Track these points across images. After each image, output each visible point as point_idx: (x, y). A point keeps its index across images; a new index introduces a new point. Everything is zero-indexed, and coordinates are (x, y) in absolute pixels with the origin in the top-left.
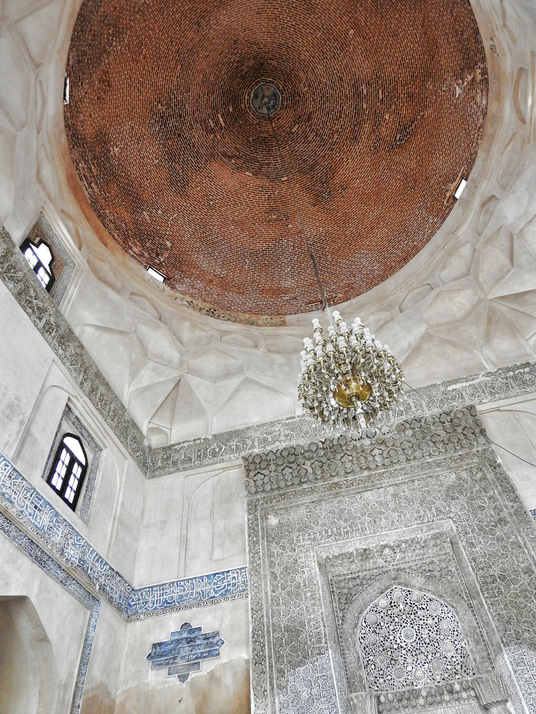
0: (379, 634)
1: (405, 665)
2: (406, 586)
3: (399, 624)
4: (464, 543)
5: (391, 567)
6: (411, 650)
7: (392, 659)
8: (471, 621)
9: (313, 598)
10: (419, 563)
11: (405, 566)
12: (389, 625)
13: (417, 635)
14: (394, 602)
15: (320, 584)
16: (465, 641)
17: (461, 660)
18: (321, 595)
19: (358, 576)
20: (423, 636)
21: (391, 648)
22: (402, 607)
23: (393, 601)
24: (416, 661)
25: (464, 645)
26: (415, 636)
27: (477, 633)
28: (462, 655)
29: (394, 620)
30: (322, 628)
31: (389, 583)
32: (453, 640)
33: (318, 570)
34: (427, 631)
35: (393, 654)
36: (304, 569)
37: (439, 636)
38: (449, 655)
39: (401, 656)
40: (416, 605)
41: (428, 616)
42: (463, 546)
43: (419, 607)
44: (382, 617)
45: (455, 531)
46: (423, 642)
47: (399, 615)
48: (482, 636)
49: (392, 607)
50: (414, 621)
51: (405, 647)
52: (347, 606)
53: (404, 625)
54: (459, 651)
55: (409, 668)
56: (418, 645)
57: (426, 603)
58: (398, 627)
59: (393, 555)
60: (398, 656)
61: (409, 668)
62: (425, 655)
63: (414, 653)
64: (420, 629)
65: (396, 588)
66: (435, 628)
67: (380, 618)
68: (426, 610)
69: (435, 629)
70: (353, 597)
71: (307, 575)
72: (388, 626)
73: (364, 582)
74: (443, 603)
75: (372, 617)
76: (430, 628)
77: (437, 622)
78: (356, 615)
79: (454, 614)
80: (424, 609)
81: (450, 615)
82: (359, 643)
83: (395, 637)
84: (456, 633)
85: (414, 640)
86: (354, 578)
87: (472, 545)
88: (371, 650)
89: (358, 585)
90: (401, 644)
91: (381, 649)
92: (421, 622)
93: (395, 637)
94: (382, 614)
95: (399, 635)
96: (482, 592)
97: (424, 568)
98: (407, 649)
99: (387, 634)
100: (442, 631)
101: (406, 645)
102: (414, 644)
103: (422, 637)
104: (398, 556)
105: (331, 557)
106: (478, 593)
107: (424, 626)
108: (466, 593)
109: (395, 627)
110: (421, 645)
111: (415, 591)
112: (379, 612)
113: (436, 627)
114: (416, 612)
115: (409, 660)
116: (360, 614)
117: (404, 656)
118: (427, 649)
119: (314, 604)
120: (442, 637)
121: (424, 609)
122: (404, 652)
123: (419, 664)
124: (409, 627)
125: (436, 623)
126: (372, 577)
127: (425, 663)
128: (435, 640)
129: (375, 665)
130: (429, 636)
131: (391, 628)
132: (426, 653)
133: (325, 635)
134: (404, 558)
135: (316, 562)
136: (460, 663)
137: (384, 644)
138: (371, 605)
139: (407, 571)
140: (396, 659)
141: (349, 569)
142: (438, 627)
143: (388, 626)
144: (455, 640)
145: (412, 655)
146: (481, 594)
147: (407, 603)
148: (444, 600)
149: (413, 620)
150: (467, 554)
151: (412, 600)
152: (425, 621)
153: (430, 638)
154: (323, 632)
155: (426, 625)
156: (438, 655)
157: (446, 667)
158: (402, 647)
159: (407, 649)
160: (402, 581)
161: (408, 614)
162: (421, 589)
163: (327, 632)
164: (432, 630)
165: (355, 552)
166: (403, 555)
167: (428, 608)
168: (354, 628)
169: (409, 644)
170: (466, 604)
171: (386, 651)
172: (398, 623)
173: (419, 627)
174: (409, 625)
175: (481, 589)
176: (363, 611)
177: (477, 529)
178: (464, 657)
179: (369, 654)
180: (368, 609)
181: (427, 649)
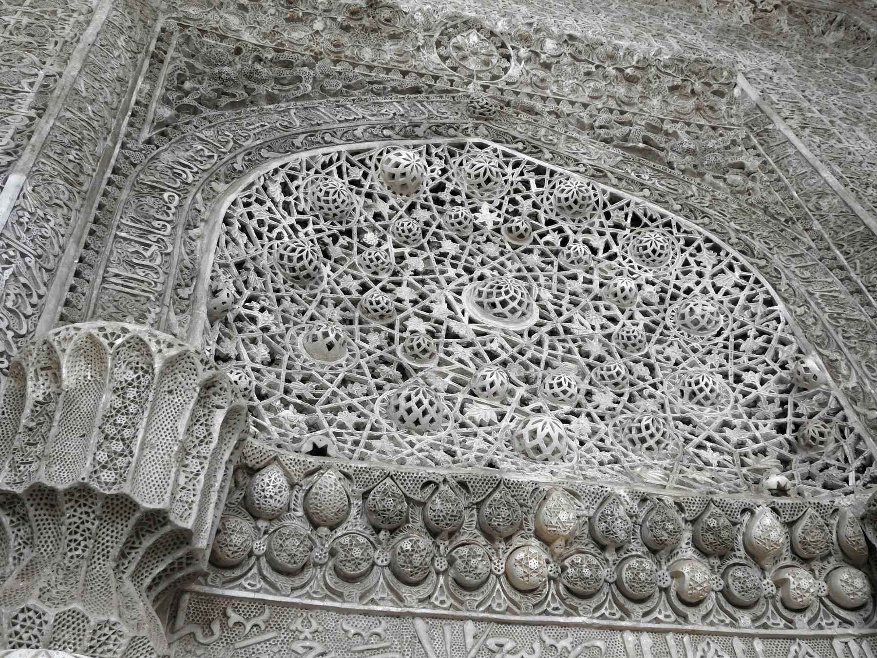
2: (536, 151)
23: (450, 186)
32: (731, 368)
37: (659, 347)
40: (560, 230)
44: (378, 216)
49: (439, 202)
65: (481, 146)
68: (601, 255)
72: (400, 258)
90: (455, 327)
112: (369, 195)
116: (270, 148)
131: (417, 263)
140: (406, 362)
142: (655, 317)
144: (747, 370)
158: (450, 335)
159: (482, 350)
167: (615, 249)
176: (294, 149)
180: (320, 154)
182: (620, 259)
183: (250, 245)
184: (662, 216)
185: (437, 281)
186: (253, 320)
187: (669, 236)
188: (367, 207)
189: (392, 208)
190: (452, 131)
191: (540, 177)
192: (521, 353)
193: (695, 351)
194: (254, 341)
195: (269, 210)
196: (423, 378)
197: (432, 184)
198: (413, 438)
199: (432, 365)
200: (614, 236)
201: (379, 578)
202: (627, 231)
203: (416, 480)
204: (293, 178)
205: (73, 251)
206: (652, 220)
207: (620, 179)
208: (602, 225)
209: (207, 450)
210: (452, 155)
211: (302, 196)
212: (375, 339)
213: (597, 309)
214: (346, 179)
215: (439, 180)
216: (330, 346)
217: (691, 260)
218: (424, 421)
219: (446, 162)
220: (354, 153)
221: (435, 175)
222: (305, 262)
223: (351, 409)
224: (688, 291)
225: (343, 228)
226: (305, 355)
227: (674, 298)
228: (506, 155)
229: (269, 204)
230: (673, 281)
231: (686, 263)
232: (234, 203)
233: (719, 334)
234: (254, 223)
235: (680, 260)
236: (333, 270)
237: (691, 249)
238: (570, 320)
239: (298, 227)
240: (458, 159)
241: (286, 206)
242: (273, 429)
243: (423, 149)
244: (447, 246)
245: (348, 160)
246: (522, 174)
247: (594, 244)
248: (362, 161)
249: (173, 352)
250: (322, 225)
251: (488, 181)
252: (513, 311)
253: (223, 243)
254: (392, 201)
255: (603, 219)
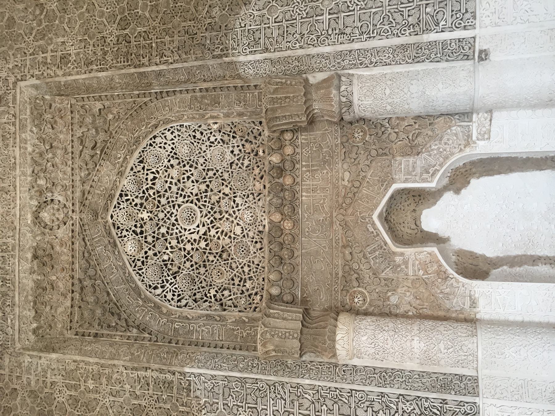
0: (179, 268)
1: (233, 236)
2: (111, 197)
3: (171, 227)
4: (60, 72)
5: (76, 216)
6: (212, 218)
7: (220, 256)
8: (182, 101)
9: (97, 377)
10: (79, 162)
11: (78, 190)
12: (169, 246)
13: (192, 202)
14: (136, 226)
15: (78, 358)
16: (211, 121)
17: (238, 138)
18: (96, 360)
19: (80, 281)
20: (194, 192)
21: (205, 253)
22: (145, 215)
23: (133, 228)
24: (230, 215)
25: (215, 127)
26: (193, 205)
27: (203, 97)
28: (231, 134)
29: (163, 235)
30: (149, 373)
31: (101, 227)
32: (208, 143)
33: (54, 356)
34: (189, 184)
35: (214, 251)
36: (49, 380)
37: (199, 165)
38: (229, 157)
39: (219, 238)
40: (147, 189)
41: (166, 174)
42: (64, 75)
43: (150, 185)
44: (155, 255)
45: (38, 82)
46: (203, 195)
47: (158, 225)
48: (207, 90)
50: (170, 200)
51: (205, 228)
52: (124, 316)
53: (173, 219)
54: (226, 138)
55: (238, 230)
56: (207, 204)
57: (146, 172)
58: (175, 231)
59: (56, 206)
60: (217, 245)
61: (238, 230)
62: (223, 198)
63: (218, 216)
64: (183, 194)
66: (185, 168)
67: (156, 258)
68: (157, 175)
69: (187, 168)
70: (111, 300)
71: (58, 379)
72: (172, 247)
73: (91, 272)
74: (147, 141)
75: (151, 274)
76: (185, 176)
77: (177, 161)
78: (141, 303)
79: (168, 127)
80: (155, 178)
81: (169, 136)
82: (186, 309)
83: (189, 241)
84: (198, 135)
85: (198, 210)
86: (82, 289)
87: (65, 59)
88: (201, 290)
89: (93, 286)
90: (201, 232)
91: (202, 270)
92: (174, 188)
93: (189, 241)
94: (150, 253)
95: (187, 233)
96: (139, 66)
97: (88, 158)
98: (210, 226)
99: (183, 253)
100: (192, 158)
101: (204, 225)
102: (204, 213)
103: (197, 195)
104: (58, 197)
105: (35, 325)
106: (141, 73)
107: (181, 186)
108: (138, 96)
109: (174, 235)
110: (208, 200)
111: (121, 186)
112: (146, 258)
113: (184, 166)
114: (158, 192)
115: (225, 226)
116: (140, 295)
117: (219, 234)
118: (216, 191)
119: (109, 378)
120: (201, 160)
121: (155, 178)
122: (213, 232)
123: (234, 212)
124: (179, 213)
125: (179, 163)
126: (86, 255)
127: (234, 201)
128: (204, 174)
129: (225, 289)
130: (197, 181)
131: (174, 243)
132: (221, 195)
133: (161, 371)
134: (65, 188)
135: (41, 354)
136: (243, 142)
137: (196, 263)
138: (131, 270)
139: (88, 188)
140: (220, 250)
141: (64, 295)
142: (185, 162)
143: (172, 247)
144: (209, 140)
145: (220, 219)
146: (142, 70)
147: (141, 205)
148: (144, 138)
149: (169, 202)
150: (78, 73)
151: (137, 194)
152: (173, 181)
153: (201, 180)
154: (155, 374)
155: (179, 181)
156: (226, 176)
157: (244, 168)
158: (205, 234)
159: (210, 226)
160: (101, 202)
161: (158, 207)
162: (121, 174)
163: (156, 366)
164: (189, 174)
165: (35, 277)
166: (59, 188)
167: (154, 170)
168: (161, 312)
169: (203, 220)
170: (155, 102)
171: (207, 263)
172: (168, 228)
173: (181, 195)
174: (174, 211)
175: (135, 67)
176: (137, 286)
177: (41, 42)
178: (234, 132)
179: (206, 295)
180: (136, 278)
181: (216, 191)
182: (158, 170)
183: (185, 298)
184: (140, 153)
185: (181, 236)
186: (215, 296)
187: (148, 151)
188: (152, 259)
189: (150, 249)
190: (107, 228)
191: (124, 195)
192: (209, 212)
193: (200, 153)
194: (223, 295)
195: (167, 292)
196: (226, 245)
197: (134, 235)
198: (252, 252)
199: (220, 242)
200: (148, 170)
201: (292, 261)
202: (146, 165)
203: (270, 255)
204: (150, 286)
205: (205, 349)
206: (141, 156)
207: (122, 166)
208: (143, 174)
209: (281, 313)
210: (118, 228)
211: (156, 282)
212: (211, 258)
213: (184, 182)
214: (142, 267)
215: (131, 232)
216: (221, 274)
217: (159, 145)
218: (247, 249)
219: (123, 230)
220: (131, 265)
221: (130, 234)
222: (189, 281)
223: (242, 268)
224: (173, 149)
225: (164, 267)
226: (223, 280)
227: (175, 154)
228: (115, 207)
229: (164, 293)
230: (168, 153)
231: (160, 147)
232: (170, 305)
233: (193, 143)
234: (175, 298)
235: (159, 149)
236: (183, 269)
237: (154, 145)
238: (192, 193)
239: (169, 282)
240: (120, 225)
241: (162, 287)
242: (255, 290)
243: (120, 239)
244: (163, 230)
245: (135, 267)
246: (123, 202)
247: (152, 177)
248: (133, 262)
249: (263, 326)
250: (165, 274)
251: (130, 215)
252: (194, 214)
253: (190, 308)
254: (147, 249)
255: (141, 173)
